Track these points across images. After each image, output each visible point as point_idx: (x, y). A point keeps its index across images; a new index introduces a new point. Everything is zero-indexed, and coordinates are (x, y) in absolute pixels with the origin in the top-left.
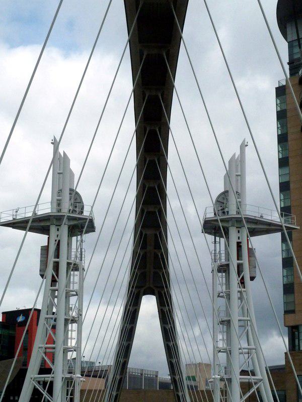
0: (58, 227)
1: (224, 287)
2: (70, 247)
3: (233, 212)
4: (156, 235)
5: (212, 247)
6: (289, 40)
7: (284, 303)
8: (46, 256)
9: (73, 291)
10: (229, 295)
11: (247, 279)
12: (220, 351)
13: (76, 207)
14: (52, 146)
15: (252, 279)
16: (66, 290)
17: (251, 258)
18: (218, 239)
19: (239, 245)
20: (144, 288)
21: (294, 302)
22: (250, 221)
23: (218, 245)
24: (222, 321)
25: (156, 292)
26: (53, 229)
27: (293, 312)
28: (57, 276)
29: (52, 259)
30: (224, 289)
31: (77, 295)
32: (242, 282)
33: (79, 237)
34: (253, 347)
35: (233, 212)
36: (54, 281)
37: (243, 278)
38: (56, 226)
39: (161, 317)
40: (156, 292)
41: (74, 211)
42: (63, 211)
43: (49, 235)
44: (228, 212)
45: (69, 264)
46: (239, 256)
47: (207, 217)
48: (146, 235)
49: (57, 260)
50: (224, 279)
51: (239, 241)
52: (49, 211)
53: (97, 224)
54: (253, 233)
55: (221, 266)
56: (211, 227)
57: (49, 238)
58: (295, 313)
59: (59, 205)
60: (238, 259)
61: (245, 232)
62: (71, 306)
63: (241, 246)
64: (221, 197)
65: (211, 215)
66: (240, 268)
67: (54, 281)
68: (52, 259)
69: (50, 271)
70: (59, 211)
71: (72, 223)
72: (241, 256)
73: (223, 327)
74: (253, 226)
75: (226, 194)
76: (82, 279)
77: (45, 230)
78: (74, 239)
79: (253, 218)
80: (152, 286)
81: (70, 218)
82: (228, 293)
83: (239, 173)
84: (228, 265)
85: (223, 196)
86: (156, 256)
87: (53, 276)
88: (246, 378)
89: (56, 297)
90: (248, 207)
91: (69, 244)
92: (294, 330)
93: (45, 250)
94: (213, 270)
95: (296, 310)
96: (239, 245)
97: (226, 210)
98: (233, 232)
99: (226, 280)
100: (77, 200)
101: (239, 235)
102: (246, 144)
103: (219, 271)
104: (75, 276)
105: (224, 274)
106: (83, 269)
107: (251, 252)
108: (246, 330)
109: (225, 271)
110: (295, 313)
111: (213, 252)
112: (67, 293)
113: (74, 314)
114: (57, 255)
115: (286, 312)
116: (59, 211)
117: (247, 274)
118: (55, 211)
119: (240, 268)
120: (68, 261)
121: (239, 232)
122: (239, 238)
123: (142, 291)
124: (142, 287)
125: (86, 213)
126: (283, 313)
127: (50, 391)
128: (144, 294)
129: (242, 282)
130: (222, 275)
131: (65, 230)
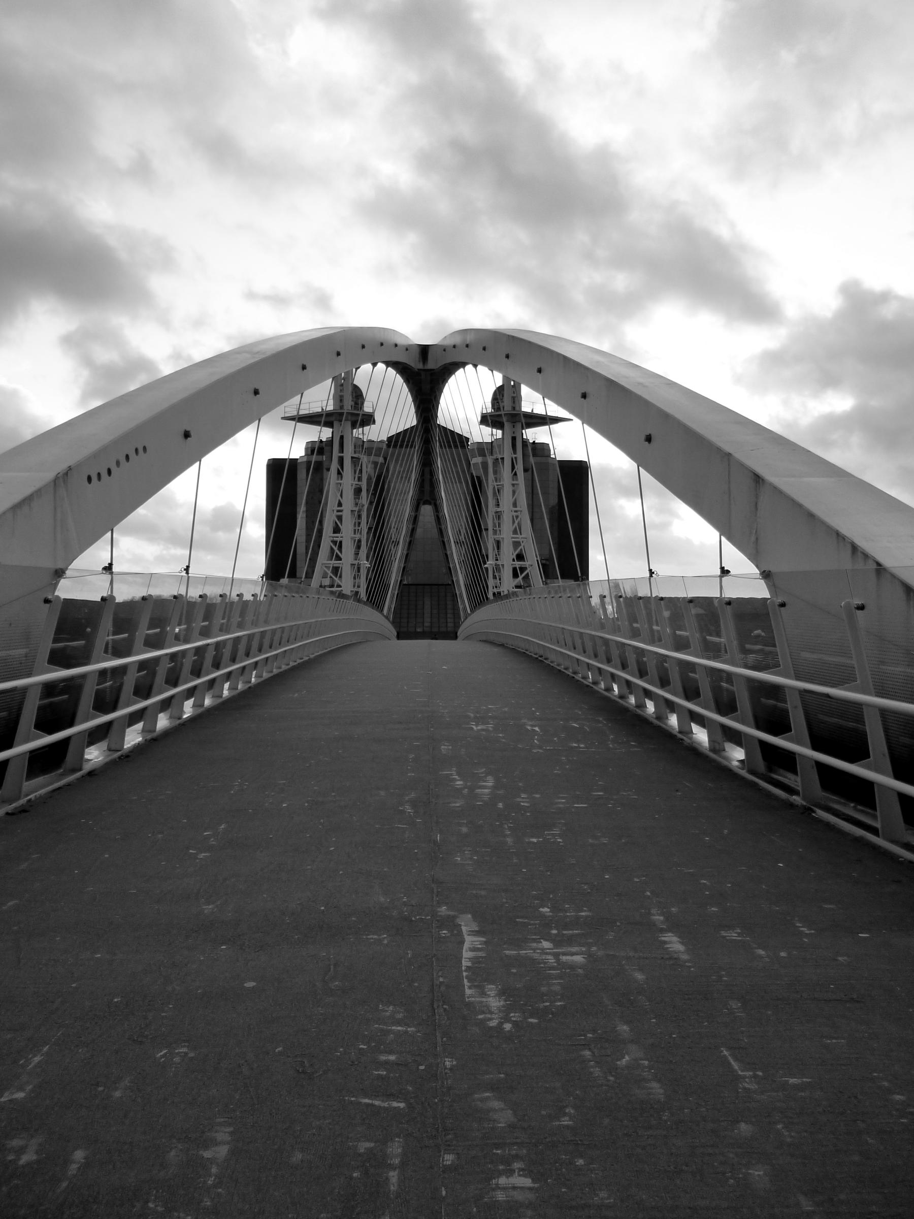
18: (494, 430)
28: (343, 470)
42: (345, 407)
43: (333, 428)
44: (503, 408)
51: (514, 435)
53: (378, 417)
57: (333, 432)
59: (341, 401)
71: (354, 418)
77: (329, 424)
78: (355, 431)
81: (352, 414)
88: (518, 564)
96: (514, 439)
98: (507, 425)
100: (358, 396)
116: (342, 407)
118: (338, 407)
122: (514, 432)
124: (421, 500)
125: (367, 408)
128: (424, 503)
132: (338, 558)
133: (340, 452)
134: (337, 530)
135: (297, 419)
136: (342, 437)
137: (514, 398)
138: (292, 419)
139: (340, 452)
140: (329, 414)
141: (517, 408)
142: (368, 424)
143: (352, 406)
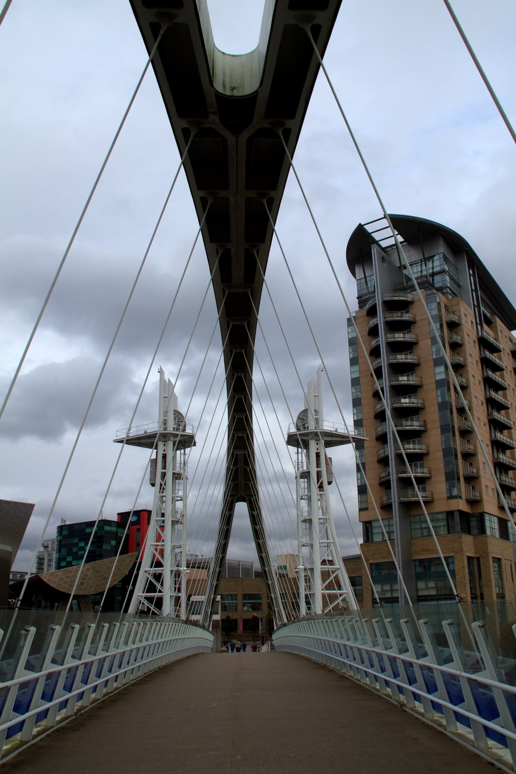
0: (165, 443)
1: (306, 490)
2: (175, 460)
3: (312, 426)
4: (245, 454)
5: (294, 457)
6: (358, 278)
7: (359, 502)
8: (154, 467)
9: (178, 497)
10: (310, 497)
11: (325, 483)
12: (303, 545)
13: (179, 425)
14: (159, 374)
15: (330, 483)
16: (172, 496)
17: (327, 466)
18: (300, 450)
19: (318, 455)
20: (238, 496)
21: (367, 501)
22: (326, 434)
23: (300, 455)
24: (305, 520)
25: (247, 500)
26: (161, 445)
27: (366, 509)
29: (159, 470)
30: (306, 493)
31: (181, 500)
32: (321, 487)
33: (183, 451)
34: (332, 541)
35: (312, 426)
36: (162, 489)
37: (322, 483)
38: (163, 442)
39: (251, 520)
40: (247, 500)
41: (178, 429)
42: (168, 429)
44: (308, 427)
45: (174, 474)
46: (318, 465)
47: (290, 432)
48: (237, 454)
50: (306, 484)
53: (197, 439)
54: (328, 444)
55: (303, 473)
56: (292, 440)
57: (157, 452)
58: (368, 510)
60: (317, 467)
62: (176, 510)
63: (319, 456)
64: (302, 414)
65: (293, 430)
66: (319, 475)
67: (162, 489)
68: (159, 470)
69: (158, 480)
70: (165, 429)
72: (320, 465)
73: (306, 525)
74: (330, 439)
75: (306, 412)
78: (178, 452)
79: (329, 432)
80: (243, 495)
82: (310, 496)
83: (317, 394)
84: (309, 472)
85: (304, 413)
86: (246, 471)
89: (164, 502)
90: (325, 423)
91: (174, 458)
92: (368, 525)
93: (154, 462)
94: (296, 477)
95: (369, 508)
96: (318, 455)
97: (306, 425)
98: (313, 444)
99: (308, 485)
101: (318, 446)
102: (322, 369)
103: (301, 477)
104: (180, 485)
105: (306, 480)
106: (186, 478)
107: (329, 461)
108: (325, 527)
109: (306, 478)
110: (368, 510)
111: (296, 461)
112: (173, 499)
113: (178, 516)
114: (164, 467)
115: (360, 510)
116: (165, 429)
117: (325, 479)
118: (162, 429)
119: (319, 475)
120: (173, 471)
121: (317, 444)
122: (318, 449)
123: (236, 498)
126: (358, 510)
128: (238, 501)
129: (321, 487)
130: (304, 481)
131: (170, 444)
132: (159, 564)
133: (162, 469)
134: (159, 538)
135: (125, 442)
136: (164, 456)
137: (317, 419)
138: (121, 441)
139: (162, 469)
140: (153, 436)
141: (320, 428)
142: (189, 446)
143: (174, 428)
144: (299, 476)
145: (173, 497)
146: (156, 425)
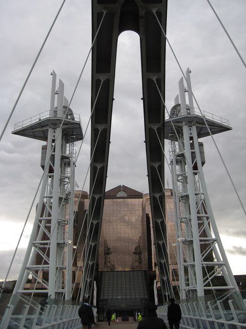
11: (199, 164)
15: (203, 163)
32: (195, 168)
37: (196, 163)
49: (53, 153)
52: (48, 116)
61: (194, 129)
66: (193, 155)
69: (47, 162)
76: (73, 172)
87: (50, 167)
93: (44, 148)
94: (172, 162)
98: (185, 129)
107: (201, 145)
112: (61, 180)
117: (198, 159)
127: (48, 255)
129: (195, 168)
131: (59, 133)
144: (174, 162)
145: (62, 177)
146: (48, 112)
